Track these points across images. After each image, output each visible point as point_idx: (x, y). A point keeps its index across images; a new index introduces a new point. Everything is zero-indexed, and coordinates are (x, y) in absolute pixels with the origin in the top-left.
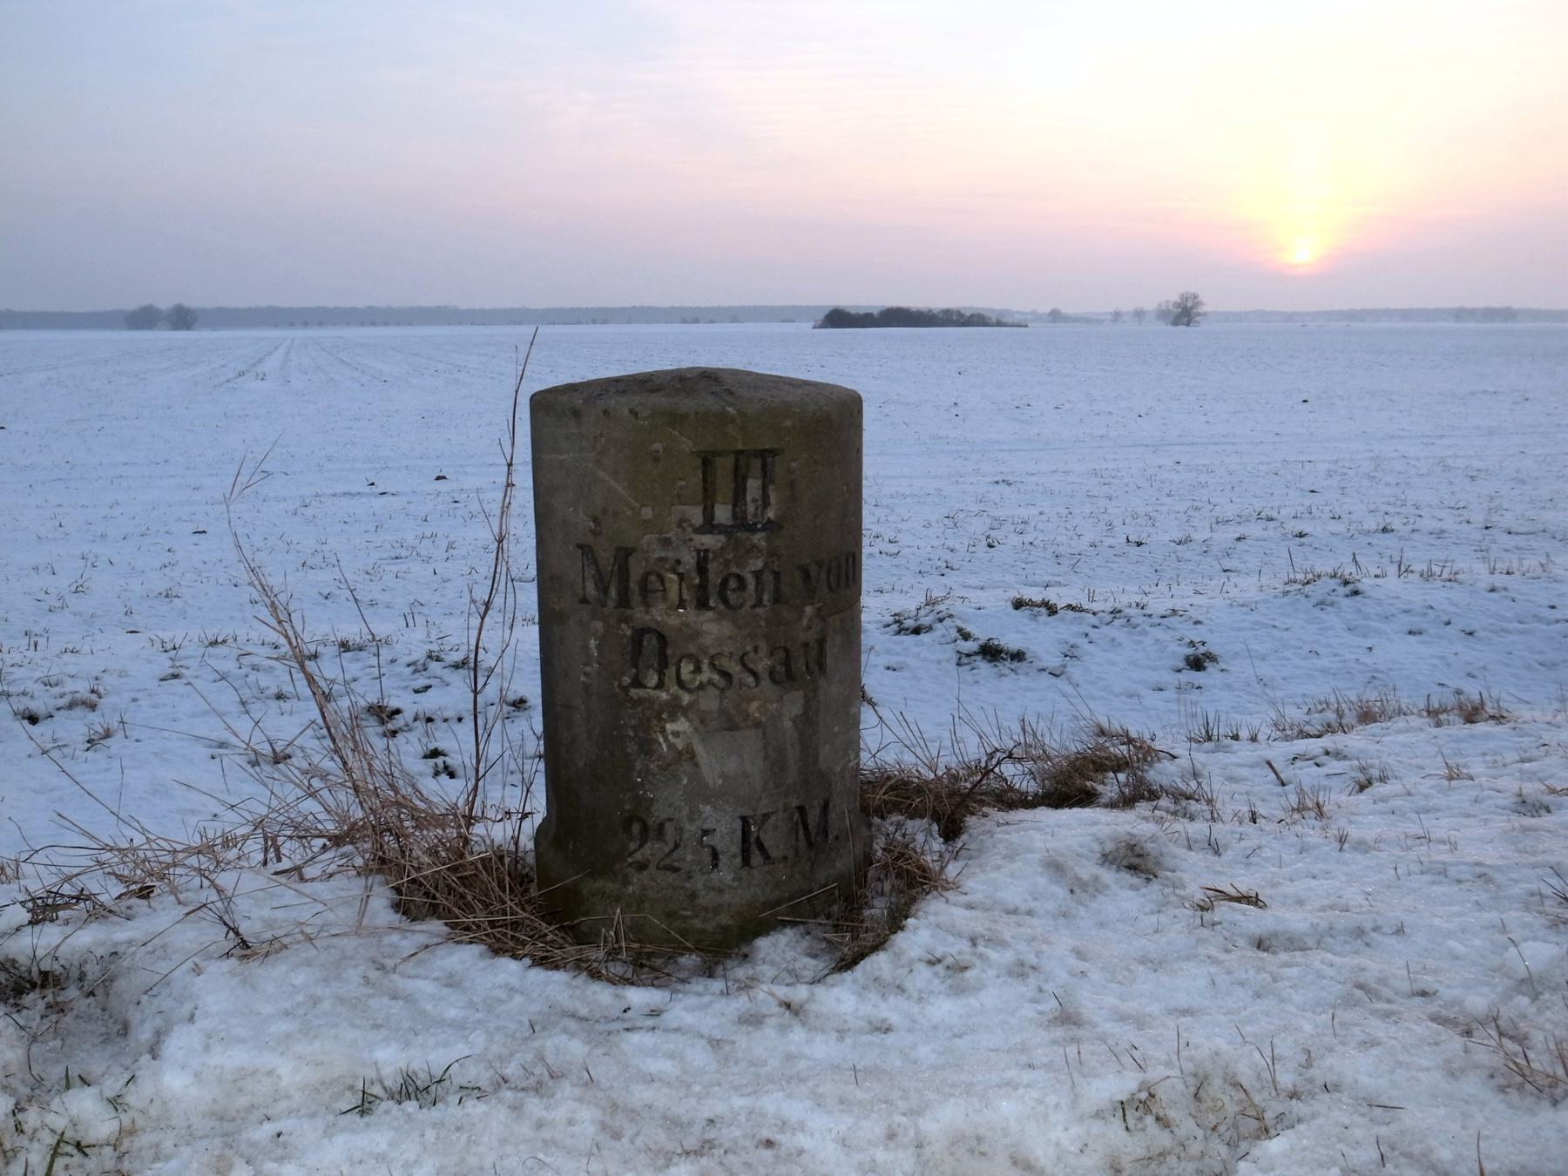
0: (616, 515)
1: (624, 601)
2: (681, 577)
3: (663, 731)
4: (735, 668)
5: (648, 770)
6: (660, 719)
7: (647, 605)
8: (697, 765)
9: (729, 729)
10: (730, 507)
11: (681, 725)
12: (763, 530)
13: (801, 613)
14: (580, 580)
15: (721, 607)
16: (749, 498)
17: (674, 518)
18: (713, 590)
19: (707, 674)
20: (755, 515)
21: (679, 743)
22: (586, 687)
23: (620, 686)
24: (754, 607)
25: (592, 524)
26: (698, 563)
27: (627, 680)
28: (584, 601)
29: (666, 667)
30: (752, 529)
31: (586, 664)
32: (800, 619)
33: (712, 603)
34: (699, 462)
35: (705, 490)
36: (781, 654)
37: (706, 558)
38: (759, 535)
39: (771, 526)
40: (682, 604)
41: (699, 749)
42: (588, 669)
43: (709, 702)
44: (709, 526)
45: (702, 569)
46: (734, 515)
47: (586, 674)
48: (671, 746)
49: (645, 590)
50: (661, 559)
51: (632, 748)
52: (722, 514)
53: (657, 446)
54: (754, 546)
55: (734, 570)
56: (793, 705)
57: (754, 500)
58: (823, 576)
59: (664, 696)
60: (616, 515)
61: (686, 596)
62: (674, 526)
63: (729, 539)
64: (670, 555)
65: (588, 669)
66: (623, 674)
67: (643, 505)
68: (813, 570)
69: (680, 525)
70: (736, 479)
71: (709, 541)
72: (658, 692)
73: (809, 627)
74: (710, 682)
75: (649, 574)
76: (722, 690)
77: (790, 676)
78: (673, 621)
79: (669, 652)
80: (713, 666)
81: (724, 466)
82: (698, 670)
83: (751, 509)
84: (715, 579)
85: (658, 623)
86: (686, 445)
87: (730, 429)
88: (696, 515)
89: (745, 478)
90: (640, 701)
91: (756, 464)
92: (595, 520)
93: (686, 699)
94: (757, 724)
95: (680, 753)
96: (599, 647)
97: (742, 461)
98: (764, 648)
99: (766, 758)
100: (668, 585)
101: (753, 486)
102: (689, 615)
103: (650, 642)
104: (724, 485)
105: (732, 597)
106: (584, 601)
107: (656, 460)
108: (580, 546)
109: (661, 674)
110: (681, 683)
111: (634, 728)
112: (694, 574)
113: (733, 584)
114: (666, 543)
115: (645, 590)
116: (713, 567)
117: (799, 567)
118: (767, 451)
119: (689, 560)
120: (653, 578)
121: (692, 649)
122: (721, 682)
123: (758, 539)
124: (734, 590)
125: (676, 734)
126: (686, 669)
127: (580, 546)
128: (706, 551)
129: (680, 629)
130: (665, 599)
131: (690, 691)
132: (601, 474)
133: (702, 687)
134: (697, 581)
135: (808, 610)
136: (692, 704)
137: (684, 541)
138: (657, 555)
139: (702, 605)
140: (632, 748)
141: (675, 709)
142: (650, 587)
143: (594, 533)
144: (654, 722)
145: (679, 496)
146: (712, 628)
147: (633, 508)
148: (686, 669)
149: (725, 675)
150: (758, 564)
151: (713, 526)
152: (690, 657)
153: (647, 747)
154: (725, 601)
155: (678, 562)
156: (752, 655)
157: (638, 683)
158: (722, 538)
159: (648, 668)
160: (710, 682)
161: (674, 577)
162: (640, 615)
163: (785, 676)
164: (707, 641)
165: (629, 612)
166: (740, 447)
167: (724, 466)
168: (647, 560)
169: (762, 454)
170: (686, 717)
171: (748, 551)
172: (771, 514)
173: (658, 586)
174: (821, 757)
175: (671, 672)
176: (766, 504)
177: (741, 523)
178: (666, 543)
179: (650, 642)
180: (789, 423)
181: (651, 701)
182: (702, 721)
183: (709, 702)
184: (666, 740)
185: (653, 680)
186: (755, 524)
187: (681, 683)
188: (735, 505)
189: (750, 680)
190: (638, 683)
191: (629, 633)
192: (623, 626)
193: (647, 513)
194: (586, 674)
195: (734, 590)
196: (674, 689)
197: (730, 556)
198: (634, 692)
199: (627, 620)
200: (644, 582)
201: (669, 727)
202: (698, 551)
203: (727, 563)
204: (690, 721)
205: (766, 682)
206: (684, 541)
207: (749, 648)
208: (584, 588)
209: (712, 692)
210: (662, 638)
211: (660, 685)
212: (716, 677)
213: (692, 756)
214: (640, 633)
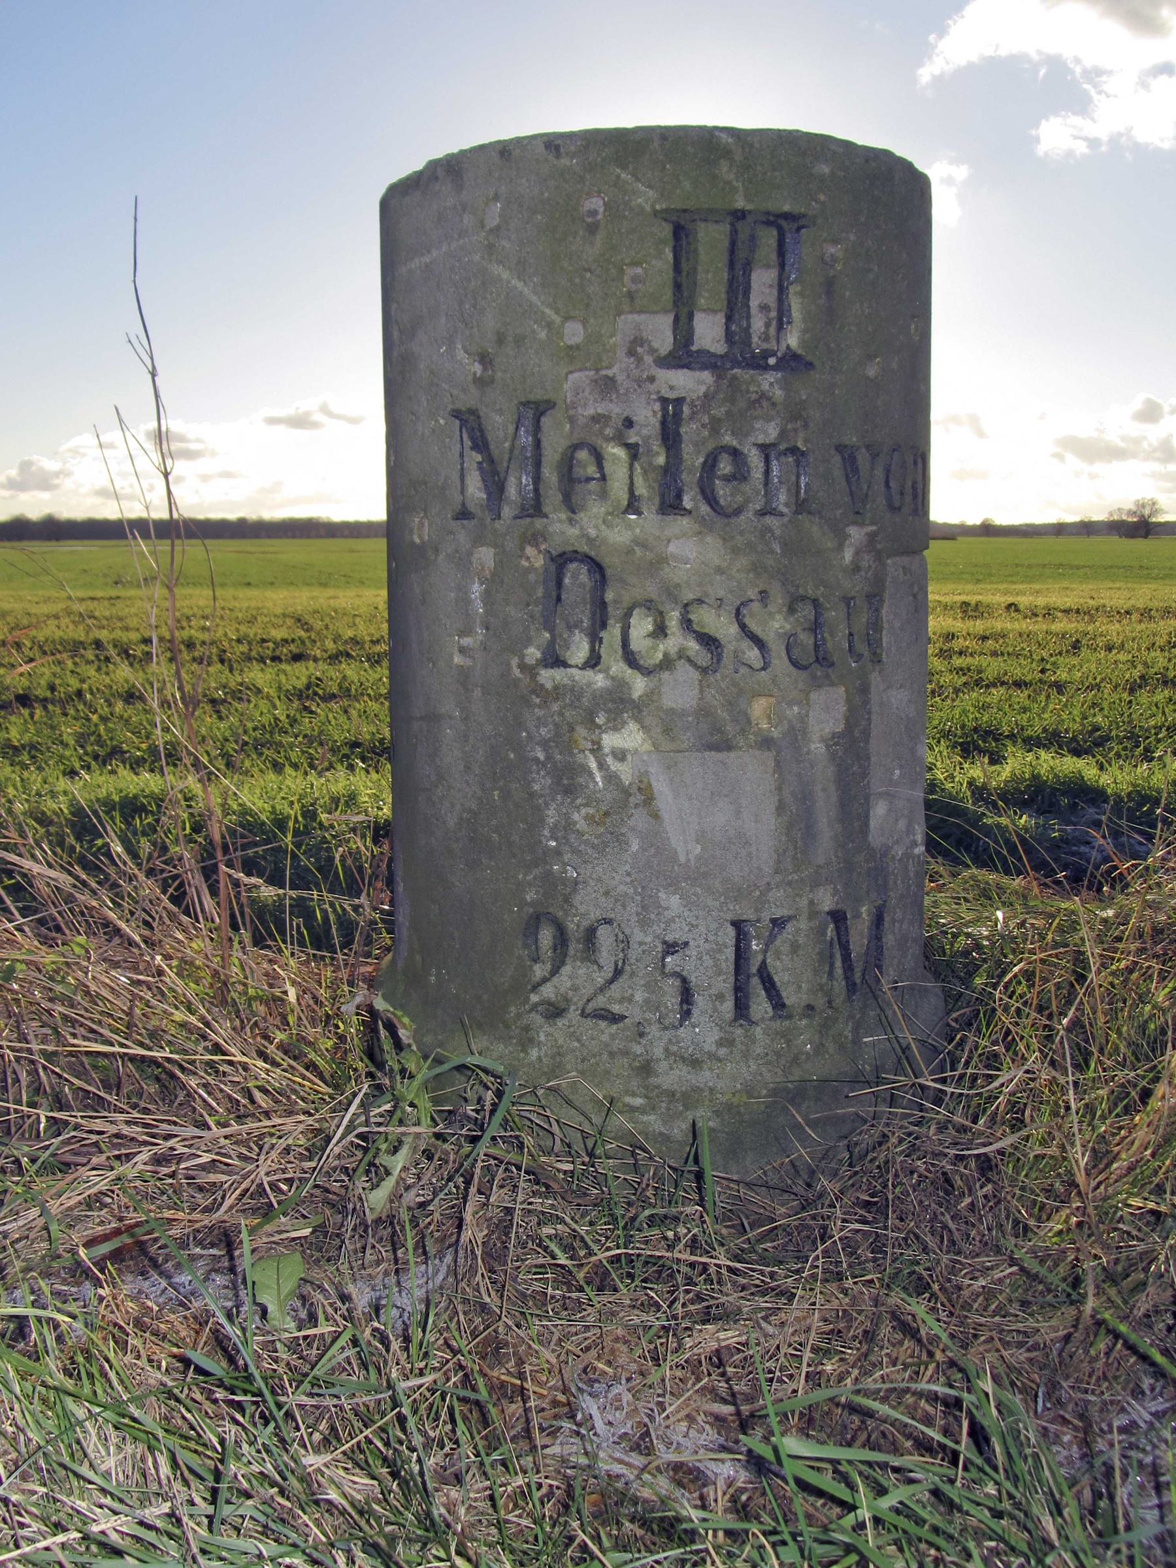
0: (520, 340)
1: (534, 508)
2: (634, 451)
3: (597, 749)
4: (723, 627)
5: (569, 825)
6: (592, 725)
7: (571, 505)
8: (656, 816)
9: (716, 747)
10: (720, 318)
11: (629, 737)
12: (775, 368)
13: (841, 538)
14: (455, 477)
15: (705, 509)
16: (754, 303)
17: (619, 340)
18: (689, 478)
19: (676, 640)
20: (766, 338)
21: (625, 772)
22: (464, 675)
23: (523, 667)
24: (762, 513)
25: (477, 368)
26: (663, 423)
27: (533, 653)
28: (464, 514)
29: (604, 625)
30: (758, 363)
31: (462, 633)
32: (840, 547)
33: (687, 503)
34: (667, 230)
35: (678, 286)
36: (806, 612)
37: (677, 414)
38: (771, 377)
39: (792, 362)
40: (633, 505)
41: (661, 786)
42: (467, 641)
43: (681, 691)
44: (683, 355)
45: (670, 435)
46: (729, 336)
47: (463, 650)
48: (611, 778)
49: (569, 478)
50: (596, 419)
51: (541, 783)
52: (708, 332)
53: (596, 203)
54: (763, 395)
55: (728, 439)
56: (826, 713)
57: (764, 308)
58: (879, 473)
59: (599, 680)
60: (520, 340)
61: (641, 489)
62: (621, 353)
63: (720, 377)
64: (615, 409)
65: (467, 641)
66: (528, 642)
67: (567, 318)
68: (863, 457)
69: (631, 353)
70: (732, 265)
71: (687, 383)
72: (589, 673)
73: (856, 568)
74: (682, 654)
75: (576, 447)
76: (704, 671)
77: (822, 658)
78: (618, 535)
79: (609, 596)
80: (687, 624)
81: (711, 239)
82: (660, 631)
83: (758, 324)
84: (693, 458)
85: (591, 541)
86: (645, 198)
87: (725, 170)
88: (660, 332)
89: (748, 267)
90: (558, 692)
91: (768, 239)
92: (485, 359)
93: (639, 685)
94: (766, 743)
95: (626, 792)
96: (487, 596)
97: (744, 230)
98: (778, 599)
99: (780, 808)
100: (608, 467)
101: (762, 282)
102: (647, 523)
103: (577, 578)
104: (711, 276)
105: (722, 491)
106: (464, 514)
107: (593, 229)
108: (456, 414)
109: (595, 639)
110: (631, 659)
111: (545, 744)
112: (656, 446)
113: (725, 466)
114: (607, 386)
115: (569, 478)
116: (688, 430)
117: (840, 448)
118: (787, 216)
119: (647, 417)
120: (583, 455)
121: (651, 590)
122: (704, 658)
123: (769, 382)
124: (727, 479)
125: (620, 755)
126: (641, 626)
127: (456, 414)
128: (679, 401)
129: (630, 552)
130: (604, 495)
131: (647, 672)
132: (497, 270)
133: (667, 664)
134: (661, 460)
135: (856, 534)
136: (651, 696)
137: (639, 382)
138: (591, 411)
139: (671, 505)
140: (541, 783)
141: (618, 705)
142: (578, 472)
143: (481, 383)
144: (581, 731)
145: (631, 296)
146: (689, 550)
147: (549, 325)
148: (641, 626)
149: (709, 641)
150: (769, 431)
151: (690, 354)
152: (648, 605)
153: (568, 781)
154: (711, 499)
155: (629, 423)
156: (756, 606)
157: (555, 660)
158: (707, 376)
159: (570, 628)
160: (682, 654)
161: (620, 452)
162: (561, 529)
163: (815, 662)
164: (678, 574)
165: (539, 523)
166: (740, 203)
167: (711, 239)
168: (572, 420)
169: (776, 220)
170: (638, 720)
171: (753, 404)
172: (792, 340)
173: (591, 470)
174: (873, 824)
175: (612, 635)
176: (782, 319)
177: (741, 355)
178: (607, 386)
179: (577, 578)
180: (825, 169)
181: (575, 692)
182: (667, 731)
183: (681, 691)
184: (602, 766)
185: (580, 650)
186: (766, 354)
187: (631, 659)
188: (729, 319)
189: (753, 655)
190: (555, 660)
191: (539, 562)
192: (530, 551)
193: (574, 333)
194: (463, 650)
195: (727, 479)
196: (618, 667)
197: (719, 411)
198: (549, 677)
199: (534, 539)
200: (567, 465)
201: (610, 741)
202: (664, 401)
203: (715, 427)
204: (644, 728)
205: (780, 662)
206: (639, 382)
207: (752, 593)
208: (463, 491)
209: (685, 674)
210: (597, 568)
211: (593, 661)
212: (693, 645)
213: (648, 796)
214: (561, 561)
